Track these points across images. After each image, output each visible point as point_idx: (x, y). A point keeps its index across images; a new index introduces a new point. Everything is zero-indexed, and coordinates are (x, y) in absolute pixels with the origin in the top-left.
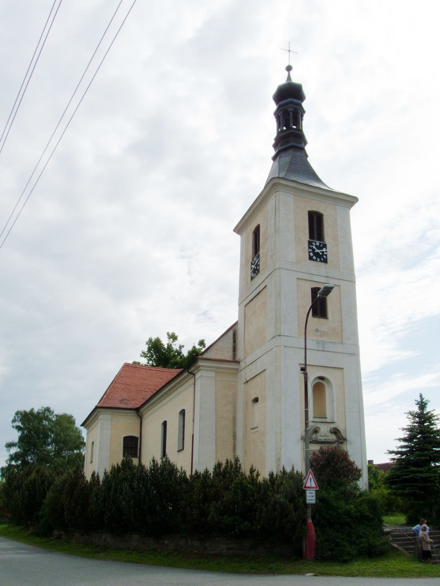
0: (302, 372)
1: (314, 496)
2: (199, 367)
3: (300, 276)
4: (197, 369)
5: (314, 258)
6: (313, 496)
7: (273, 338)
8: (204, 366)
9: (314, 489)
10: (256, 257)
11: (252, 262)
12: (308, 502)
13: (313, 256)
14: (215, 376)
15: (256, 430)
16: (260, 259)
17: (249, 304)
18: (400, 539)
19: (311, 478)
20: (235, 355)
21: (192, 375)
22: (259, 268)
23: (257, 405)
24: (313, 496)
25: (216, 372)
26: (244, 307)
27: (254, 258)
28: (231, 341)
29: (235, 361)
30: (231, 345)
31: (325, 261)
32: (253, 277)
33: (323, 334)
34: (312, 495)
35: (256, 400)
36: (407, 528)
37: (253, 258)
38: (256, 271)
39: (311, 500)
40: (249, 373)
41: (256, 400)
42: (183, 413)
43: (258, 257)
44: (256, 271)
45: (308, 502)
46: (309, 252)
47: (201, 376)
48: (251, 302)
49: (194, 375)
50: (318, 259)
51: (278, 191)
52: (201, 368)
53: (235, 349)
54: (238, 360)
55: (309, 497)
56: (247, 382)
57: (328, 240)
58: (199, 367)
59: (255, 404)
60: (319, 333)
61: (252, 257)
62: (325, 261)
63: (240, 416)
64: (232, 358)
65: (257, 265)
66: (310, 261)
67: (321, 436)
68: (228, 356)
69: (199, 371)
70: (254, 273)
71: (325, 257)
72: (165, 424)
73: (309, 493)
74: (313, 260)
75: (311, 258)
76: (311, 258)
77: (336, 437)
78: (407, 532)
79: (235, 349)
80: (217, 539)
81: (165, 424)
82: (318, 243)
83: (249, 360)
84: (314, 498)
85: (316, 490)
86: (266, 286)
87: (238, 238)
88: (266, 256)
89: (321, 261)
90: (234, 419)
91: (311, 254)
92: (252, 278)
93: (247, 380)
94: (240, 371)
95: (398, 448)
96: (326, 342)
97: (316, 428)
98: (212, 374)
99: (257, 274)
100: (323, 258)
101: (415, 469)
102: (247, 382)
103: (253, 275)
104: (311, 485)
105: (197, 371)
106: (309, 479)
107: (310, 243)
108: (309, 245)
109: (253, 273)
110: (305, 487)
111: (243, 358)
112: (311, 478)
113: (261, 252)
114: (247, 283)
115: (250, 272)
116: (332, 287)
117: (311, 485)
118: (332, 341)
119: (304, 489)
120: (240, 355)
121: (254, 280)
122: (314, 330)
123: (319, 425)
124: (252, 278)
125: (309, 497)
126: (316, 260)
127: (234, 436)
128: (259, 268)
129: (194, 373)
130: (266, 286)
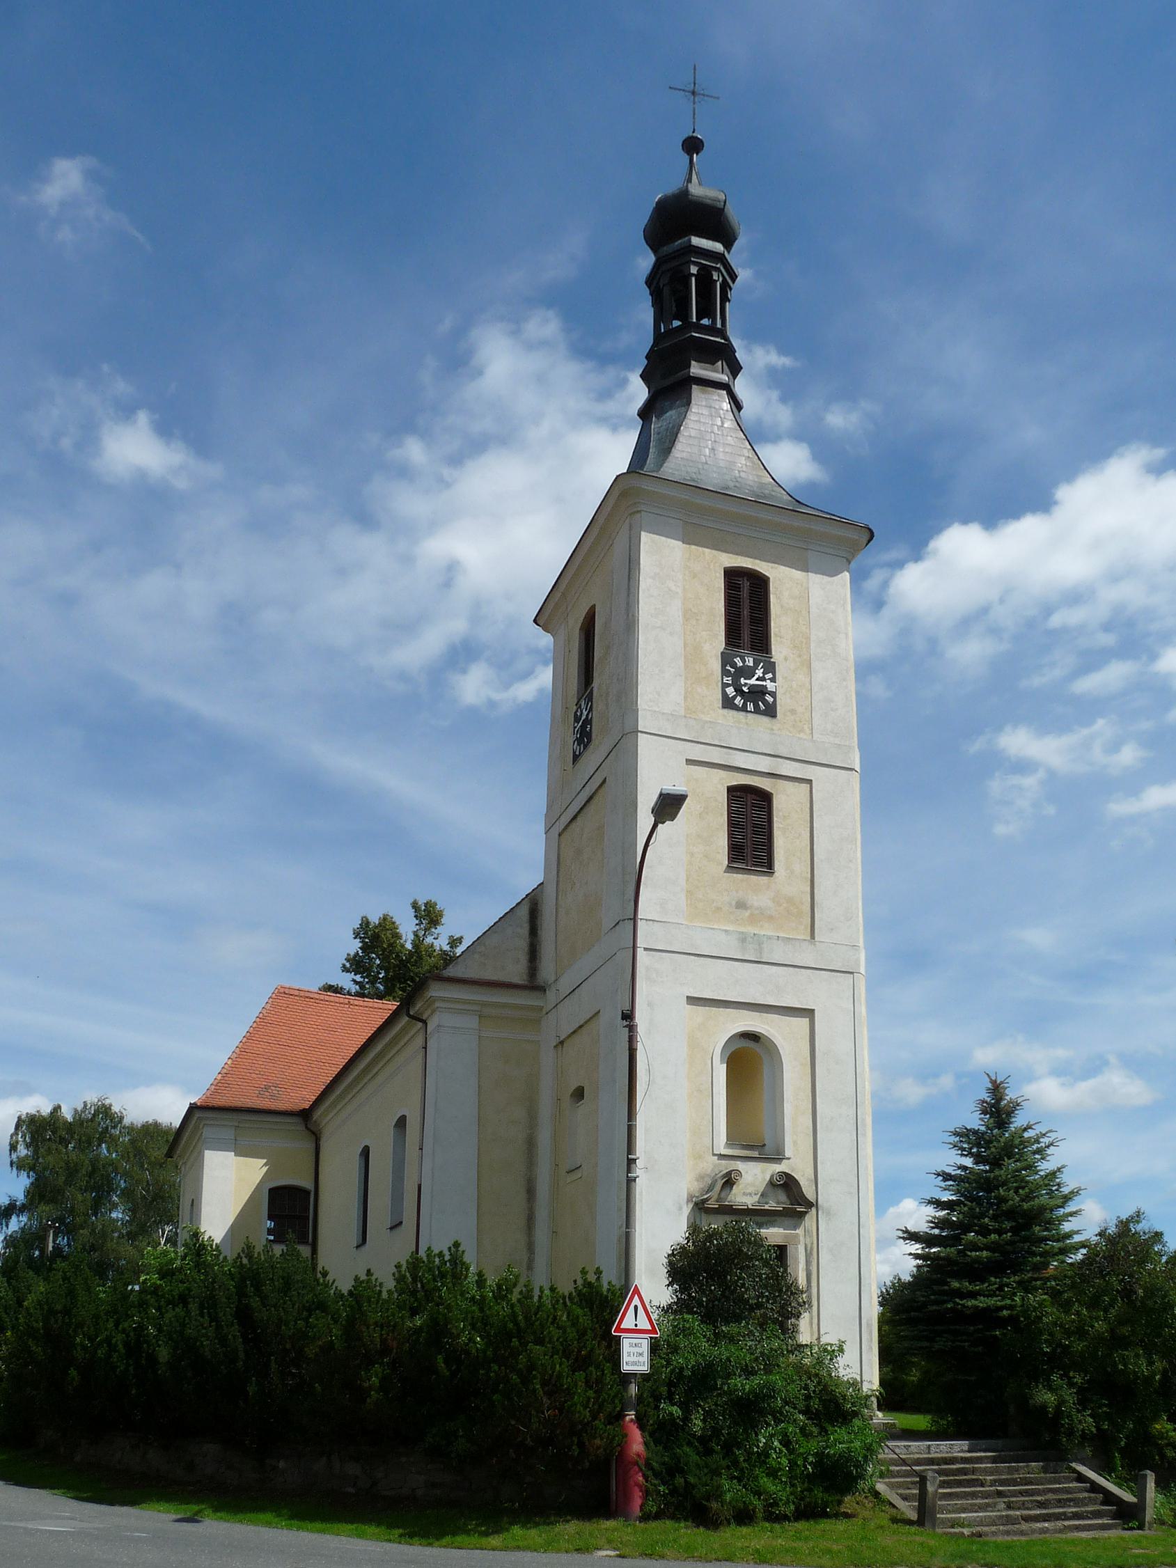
0: (625, 1023)
1: (646, 1354)
2: (432, 1001)
3: (698, 753)
4: (429, 1006)
5: (739, 701)
6: (641, 1354)
7: (617, 927)
8: (443, 999)
9: (647, 1336)
10: (585, 699)
11: (577, 711)
12: (626, 1368)
13: (734, 697)
14: (477, 1028)
15: (578, 1174)
16: (594, 706)
17: (569, 829)
18: (898, 1471)
19: (636, 1308)
20: (535, 970)
21: (420, 1024)
22: (591, 728)
23: (584, 1107)
24: (641, 1354)
25: (480, 1016)
26: (557, 836)
27: (580, 700)
28: (525, 930)
29: (533, 985)
30: (522, 944)
31: (771, 712)
32: (577, 753)
33: (759, 916)
34: (640, 1350)
35: (579, 1094)
36: (930, 1443)
37: (578, 702)
38: (584, 736)
39: (634, 1363)
40: (567, 1017)
41: (579, 1094)
42: (401, 1123)
43: (590, 698)
44: (584, 736)
45: (626, 1368)
46: (725, 686)
47: (438, 1026)
48: (573, 825)
49: (425, 1022)
50: (750, 707)
51: (638, 512)
52: (437, 1004)
53: (533, 953)
54: (543, 985)
55: (629, 1355)
56: (562, 1043)
57: (780, 649)
58: (434, 1001)
59: (579, 1104)
60: (747, 914)
61: (578, 697)
62: (771, 712)
63: (544, 1138)
64: (525, 977)
65: (588, 721)
66: (726, 711)
67: (744, 1194)
68: (515, 971)
69: (433, 1012)
70: (579, 744)
71: (769, 699)
72: (366, 1153)
73: (631, 1345)
74: (735, 708)
75: (728, 703)
76: (728, 703)
77: (788, 1197)
78: (929, 1453)
79: (533, 953)
80: (404, 1459)
81: (366, 1153)
82: (751, 660)
83: (565, 984)
84: (645, 1358)
85: (651, 1338)
86: (604, 781)
87: (545, 640)
88: (607, 694)
89: (757, 711)
90: (531, 1144)
91: (730, 691)
92: (576, 758)
93: (561, 1039)
94: (547, 1013)
95: (933, 1228)
96: (765, 939)
97: (729, 1173)
98: (472, 1022)
99: (585, 747)
100: (765, 702)
101: (967, 1286)
102: (562, 1043)
103: (578, 747)
104: (636, 1325)
105: (429, 1012)
106: (632, 1308)
107: (726, 660)
108: (723, 666)
109: (578, 744)
110: (618, 1329)
111: (553, 979)
112: (636, 1308)
113: (595, 684)
114: (564, 770)
115: (571, 739)
116: (684, 793)
117: (636, 1325)
118: (781, 935)
119: (614, 1334)
120: (547, 971)
121: (582, 760)
122: (734, 903)
123: (740, 1166)
124: (576, 758)
125: (629, 1355)
126: (744, 709)
127: (531, 1192)
128: (591, 728)
129: (424, 1018)
130: (604, 781)
